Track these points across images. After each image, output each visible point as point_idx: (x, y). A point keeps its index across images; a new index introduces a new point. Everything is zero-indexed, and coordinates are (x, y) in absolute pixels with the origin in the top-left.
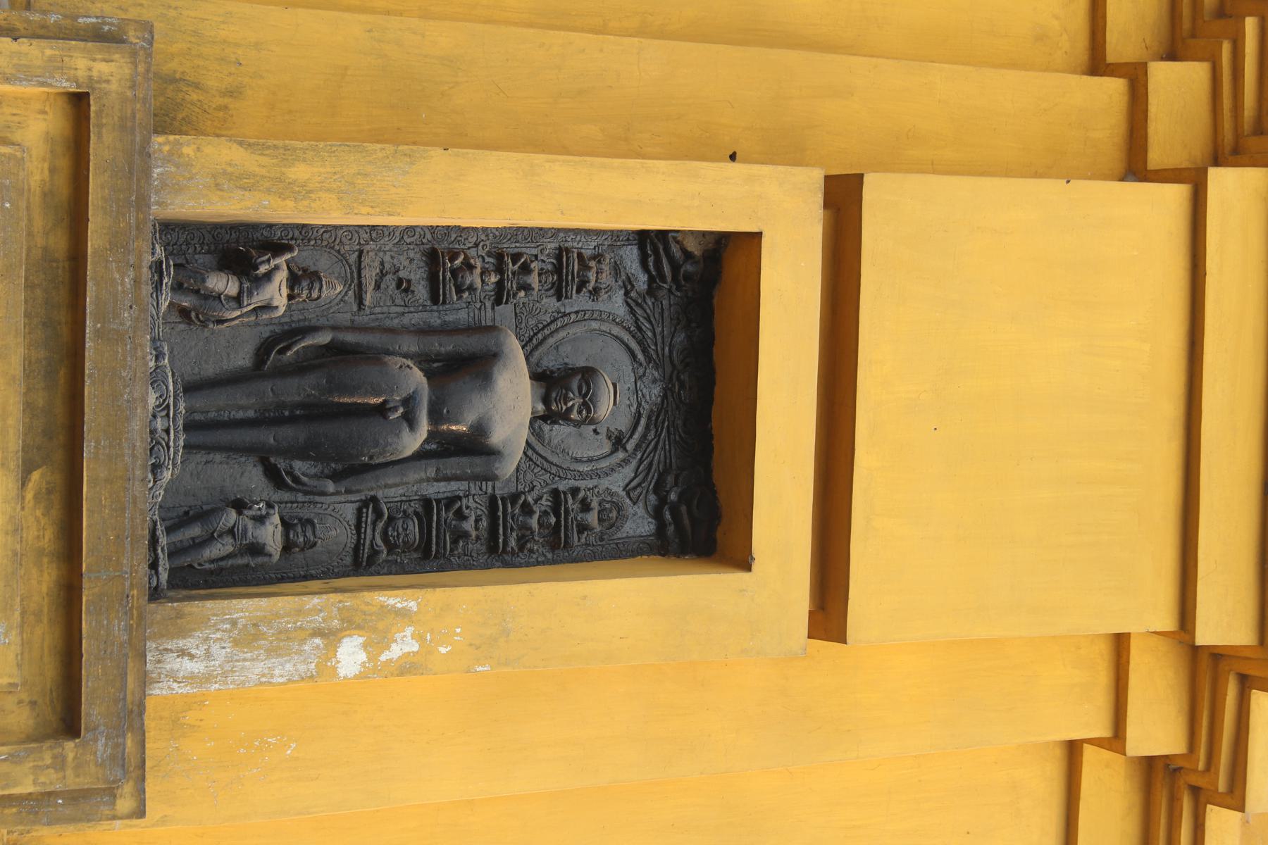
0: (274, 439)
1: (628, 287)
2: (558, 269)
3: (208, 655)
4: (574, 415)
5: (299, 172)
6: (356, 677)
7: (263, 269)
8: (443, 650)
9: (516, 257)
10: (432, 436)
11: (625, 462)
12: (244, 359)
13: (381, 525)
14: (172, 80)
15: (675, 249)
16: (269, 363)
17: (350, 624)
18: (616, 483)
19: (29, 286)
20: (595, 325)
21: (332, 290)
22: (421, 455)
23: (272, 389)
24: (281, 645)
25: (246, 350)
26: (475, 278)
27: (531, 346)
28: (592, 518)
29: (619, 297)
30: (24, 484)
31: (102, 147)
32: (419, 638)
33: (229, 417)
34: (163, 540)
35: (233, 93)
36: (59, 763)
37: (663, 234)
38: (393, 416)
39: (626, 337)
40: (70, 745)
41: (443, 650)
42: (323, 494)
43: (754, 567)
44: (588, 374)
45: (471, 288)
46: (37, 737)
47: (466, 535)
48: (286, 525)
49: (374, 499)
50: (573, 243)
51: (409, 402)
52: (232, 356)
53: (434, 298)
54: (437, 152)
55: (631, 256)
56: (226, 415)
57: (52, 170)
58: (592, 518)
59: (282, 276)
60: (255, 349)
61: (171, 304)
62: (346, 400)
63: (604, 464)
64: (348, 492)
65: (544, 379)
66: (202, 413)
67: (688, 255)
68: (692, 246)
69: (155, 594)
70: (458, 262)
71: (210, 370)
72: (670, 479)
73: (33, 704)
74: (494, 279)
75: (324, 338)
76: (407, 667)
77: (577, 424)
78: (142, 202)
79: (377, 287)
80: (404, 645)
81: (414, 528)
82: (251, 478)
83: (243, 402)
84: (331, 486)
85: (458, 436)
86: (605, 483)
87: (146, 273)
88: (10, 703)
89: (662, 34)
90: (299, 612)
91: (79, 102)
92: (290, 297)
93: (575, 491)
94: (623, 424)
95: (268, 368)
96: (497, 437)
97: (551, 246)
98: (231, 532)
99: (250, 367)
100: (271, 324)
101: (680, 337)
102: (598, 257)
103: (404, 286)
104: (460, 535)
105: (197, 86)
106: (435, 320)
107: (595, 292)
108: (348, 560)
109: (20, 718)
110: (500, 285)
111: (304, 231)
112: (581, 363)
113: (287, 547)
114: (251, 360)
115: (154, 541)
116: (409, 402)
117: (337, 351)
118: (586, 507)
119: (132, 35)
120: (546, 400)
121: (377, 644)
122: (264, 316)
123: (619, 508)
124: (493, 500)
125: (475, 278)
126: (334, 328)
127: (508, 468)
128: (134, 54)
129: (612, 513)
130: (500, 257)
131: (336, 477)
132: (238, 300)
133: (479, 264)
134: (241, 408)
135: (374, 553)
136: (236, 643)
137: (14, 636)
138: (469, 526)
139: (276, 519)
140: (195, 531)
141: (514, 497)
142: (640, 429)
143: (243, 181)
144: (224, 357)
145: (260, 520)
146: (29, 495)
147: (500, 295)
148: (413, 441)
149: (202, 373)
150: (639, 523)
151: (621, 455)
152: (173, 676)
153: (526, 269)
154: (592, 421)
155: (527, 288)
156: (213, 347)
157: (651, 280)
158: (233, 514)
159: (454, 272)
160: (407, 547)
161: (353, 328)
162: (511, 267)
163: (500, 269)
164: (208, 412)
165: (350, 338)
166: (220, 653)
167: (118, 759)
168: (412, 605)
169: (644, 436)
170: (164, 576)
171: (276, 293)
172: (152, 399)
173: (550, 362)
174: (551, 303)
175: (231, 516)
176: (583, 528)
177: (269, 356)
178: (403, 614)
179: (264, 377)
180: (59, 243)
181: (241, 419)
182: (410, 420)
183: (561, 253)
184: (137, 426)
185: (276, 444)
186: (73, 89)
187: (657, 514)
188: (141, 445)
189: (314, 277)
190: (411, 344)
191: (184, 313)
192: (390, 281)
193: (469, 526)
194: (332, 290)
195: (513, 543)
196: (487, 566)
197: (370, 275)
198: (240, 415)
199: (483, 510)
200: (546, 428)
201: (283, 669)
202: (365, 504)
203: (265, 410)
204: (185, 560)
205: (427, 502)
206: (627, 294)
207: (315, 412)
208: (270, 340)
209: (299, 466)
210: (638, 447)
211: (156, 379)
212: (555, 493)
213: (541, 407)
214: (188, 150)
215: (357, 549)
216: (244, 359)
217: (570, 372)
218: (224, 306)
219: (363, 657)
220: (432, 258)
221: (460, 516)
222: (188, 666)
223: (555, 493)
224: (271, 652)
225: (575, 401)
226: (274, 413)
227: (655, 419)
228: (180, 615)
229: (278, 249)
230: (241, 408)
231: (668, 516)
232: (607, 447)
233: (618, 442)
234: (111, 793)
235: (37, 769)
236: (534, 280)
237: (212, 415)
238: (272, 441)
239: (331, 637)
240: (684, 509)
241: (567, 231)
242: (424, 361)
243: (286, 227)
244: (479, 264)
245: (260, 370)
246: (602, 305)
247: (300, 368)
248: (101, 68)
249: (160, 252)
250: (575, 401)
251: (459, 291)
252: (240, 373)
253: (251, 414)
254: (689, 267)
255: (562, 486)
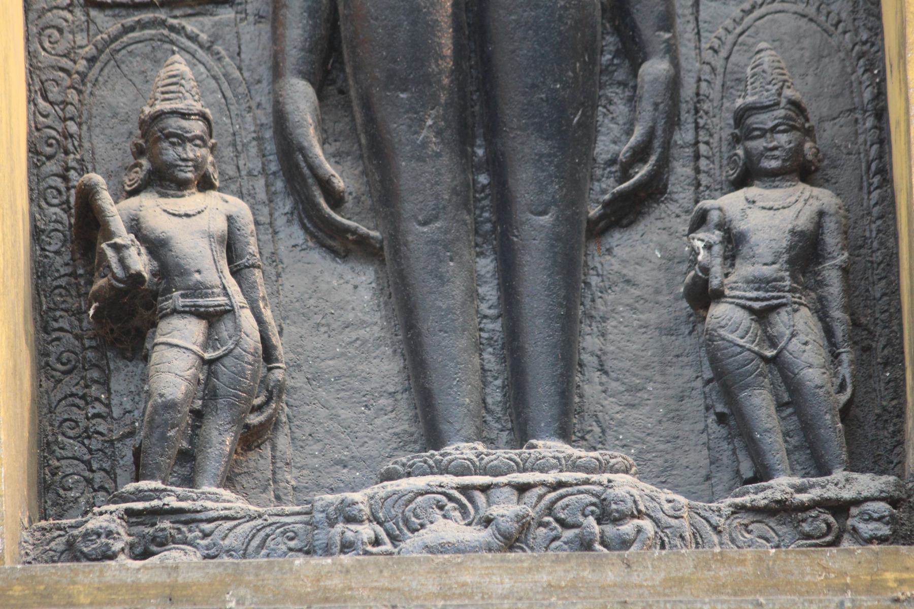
0: (544, 213)
12: (356, 287)
16: (363, 229)
23: (425, 223)
25: (335, 283)
33: (494, 319)
52: (351, 317)
56: (491, 326)
60: (334, 260)
66: (485, 383)
83: (457, 289)
95: (376, 228)
99: (376, 272)
100: (271, 224)
114: (359, 268)
122: (253, 248)
134: (473, 295)
144: (354, 336)
149: (391, 389)
156: (331, 363)
164: (483, 369)
177: (347, 230)
179: (396, 238)
181: (499, 289)
185: (553, 210)
198: (489, 291)
203: (477, 233)
208: (309, 225)
216: (356, 287)
218: (231, 351)
226: (483, 209)
230: (473, 295)
237: (490, 359)
238: (546, 219)
245: (382, 248)
252: (390, 296)
253: (486, 265)
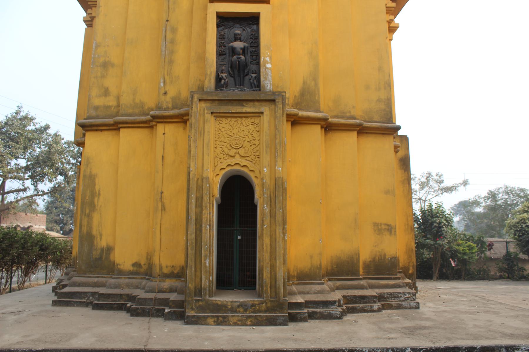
1: (224, 29)
2: (221, 38)
3: (267, 83)
4: (240, 36)
5: (209, 73)
6: (271, 65)
7: (221, 77)
8: (269, 54)
9: (220, 44)
10: (242, 55)
11: (247, 29)
13: (254, 61)
14: (199, 88)
15: (219, 23)
17: (265, 66)
18: (249, 30)
19: (222, 106)
20: (229, 33)
21: (224, 68)
22: (245, 56)
24: (267, 74)
26: (223, 49)
27: (232, 42)
28: (254, 33)
29: (225, 30)
30: (245, 106)
31: (205, 97)
32: (267, 57)
34: (254, 89)
35: (200, 80)
36: (278, 102)
37: (217, 25)
38: (239, 60)
39: (230, 29)
40: (276, 101)
41: (269, 54)
42: (249, 69)
43: (260, 11)
44: (235, 34)
45: (224, 50)
46: (275, 104)
47: (255, 50)
48: (253, 73)
49: (250, 62)
50: (218, 37)
51: (238, 58)
53: (225, 55)
54: (206, 55)
55: (220, 29)
57: (208, 103)
58: (254, 33)
59: (222, 74)
61: (225, 88)
62: (237, 66)
63: (247, 32)
64: (249, 66)
65: (236, 40)
67: (220, 21)
68: (218, 21)
69: (260, 90)
70: (220, 51)
71: (234, 83)
72: (249, 23)
73: (271, 105)
74: (223, 47)
75: (230, 69)
76: (270, 58)
77: (241, 36)
78: (212, 92)
79: (224, 62)
80: (268, 59)
81: (254, 57)
82: (247, 78)
84: (248, 68)
85: (242, 52)
86: (249, 32)
87: (221, 92)
88: (271, 107)
89: (192, 24)
90: (263, 72)
91: (200, 100)
92: (224, 73)
93: (250, 36)
94: (241, 29)
96: (242, 46)
97: (219, 39)
98: (253, 81)
101: (230, 22)
102: (220, 33)
103: (224, 59)
104: (255, 51)
105: (199, 85)
106: (228, 54)
107: (224, 33)
108: (258, 65)
109: (273, 106)
110: (224, 46)
111: (217, 71)
112: (233, 35)
113: (255, 73)
115: (254, 90)
116: (238, 58)
117: (231, 67)
118: (252, 34)
119: (192, 93)
120: (238, 40)
121: (267, 62)
123: (252, 30)
124: (251, 47)
125: (223, 49)
126: (229, 67)
127: (246, 45)
128: (194, 94)
129: (253, 31)
130: (220, 46)
131: (247, 67)
132: (225, 80)
133: (221, 49)
135: (257, 62)
136: (266, 80)
137: (263, 107)
138: (254, 50)
139: (252, 75)
140: (253, 85)
141: (251, 44)
142: (242, 27)
143: (210, 80)
145: (252, 77)
146: (247, 105)
147: (225, 46)
148: (243, 57)
150: (255, 27)
151: (246, 30)
152: (270, 88)
153: (221, 43)
154: (241, 34)
155: (224, 43)
157: (223, 26)
158: (251, 80)
159: (222, 52)
160: (256, 58)
161: (229, 65)
162: (221, 45)
163: (221, 46)
165: (230, 65)
166: (267, 82)
167: (278, 95)
168: (263, 58)
169: (243, 26)
170: (258, 89)
171: (224, 75)
172: (236, 91)
173: (233, 39)
174: (226, 39)
175: (251, 80)
176: (255, 35)
178: (264, 59)
180: (217, 102)
182: (240, 58)
183: (219, 38)
184: (239, 93)
186: (198, 101)
187: (253, 25)
188: (241, 92)
189: (222, 70)
190: (231, 58)
191: (227, 86)
192: (223, 60)
193: (254, 50)
194: (224, 68)
195: (256, 44)
196: (259, 47)
197: (222, 63)
198: (239, 79)
199: (252, 48)
200: (242, 40)
201: (270, 74)
202: (251, 64)
204: (256, 86)
205: (251, 55)
206: (225, 29)
207: (239, 70)
209: (246, 72)
210: (245, 27)
211: (234, 90)
212: (250, 38)
213: (239, 41)
214: (206, 86)
215: (256, 64)
217: (234, 37)
219: (269, 64)
220: (220, 55)
221: (253, 51)
222: (269, 86)
223: (250, 38)
224: (268, 76)
225: (238, 36)
227: (241, 25)
228: (263, 87)
229: (219, 75)
231: (254, 23)
232: (244, 31)
233: (244, 30)
234: (282, 96)
235: (279, 104)
236: (223, 42)
239: (266, 68)
240: (253, 21)
241: (217, 37)
242: (233, 56)
243: (216, 74)
244: (221, 49)
246: (226, 32)
247: (233, 72)
248: (196, 97)
249: (219, 90)
250: (238, 36)
251: (224, 51)
253: (239, 78)
254: (221, 21)
255: (249, 37)
